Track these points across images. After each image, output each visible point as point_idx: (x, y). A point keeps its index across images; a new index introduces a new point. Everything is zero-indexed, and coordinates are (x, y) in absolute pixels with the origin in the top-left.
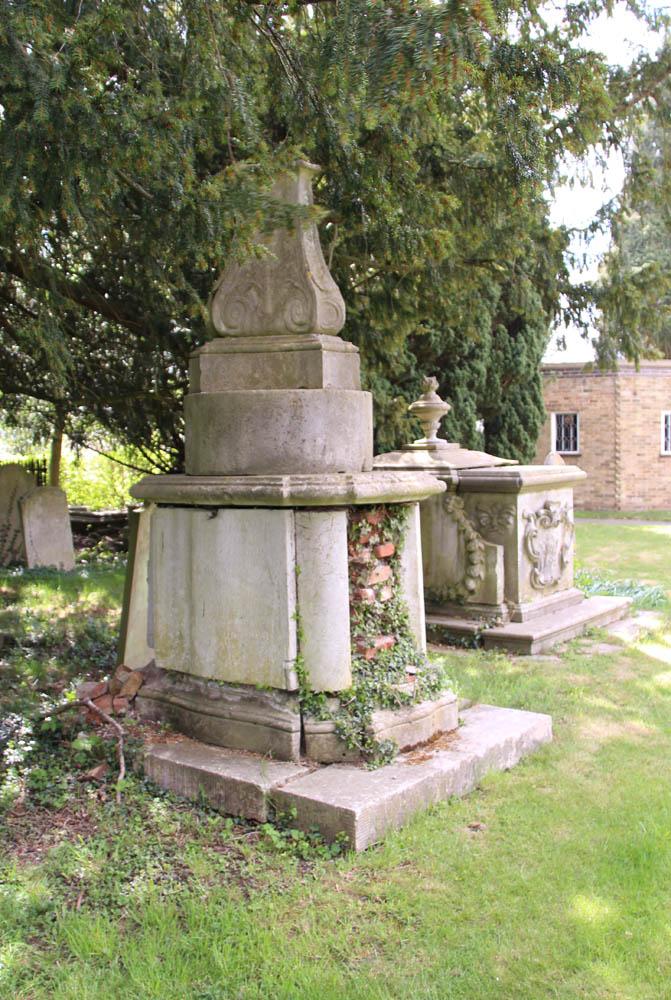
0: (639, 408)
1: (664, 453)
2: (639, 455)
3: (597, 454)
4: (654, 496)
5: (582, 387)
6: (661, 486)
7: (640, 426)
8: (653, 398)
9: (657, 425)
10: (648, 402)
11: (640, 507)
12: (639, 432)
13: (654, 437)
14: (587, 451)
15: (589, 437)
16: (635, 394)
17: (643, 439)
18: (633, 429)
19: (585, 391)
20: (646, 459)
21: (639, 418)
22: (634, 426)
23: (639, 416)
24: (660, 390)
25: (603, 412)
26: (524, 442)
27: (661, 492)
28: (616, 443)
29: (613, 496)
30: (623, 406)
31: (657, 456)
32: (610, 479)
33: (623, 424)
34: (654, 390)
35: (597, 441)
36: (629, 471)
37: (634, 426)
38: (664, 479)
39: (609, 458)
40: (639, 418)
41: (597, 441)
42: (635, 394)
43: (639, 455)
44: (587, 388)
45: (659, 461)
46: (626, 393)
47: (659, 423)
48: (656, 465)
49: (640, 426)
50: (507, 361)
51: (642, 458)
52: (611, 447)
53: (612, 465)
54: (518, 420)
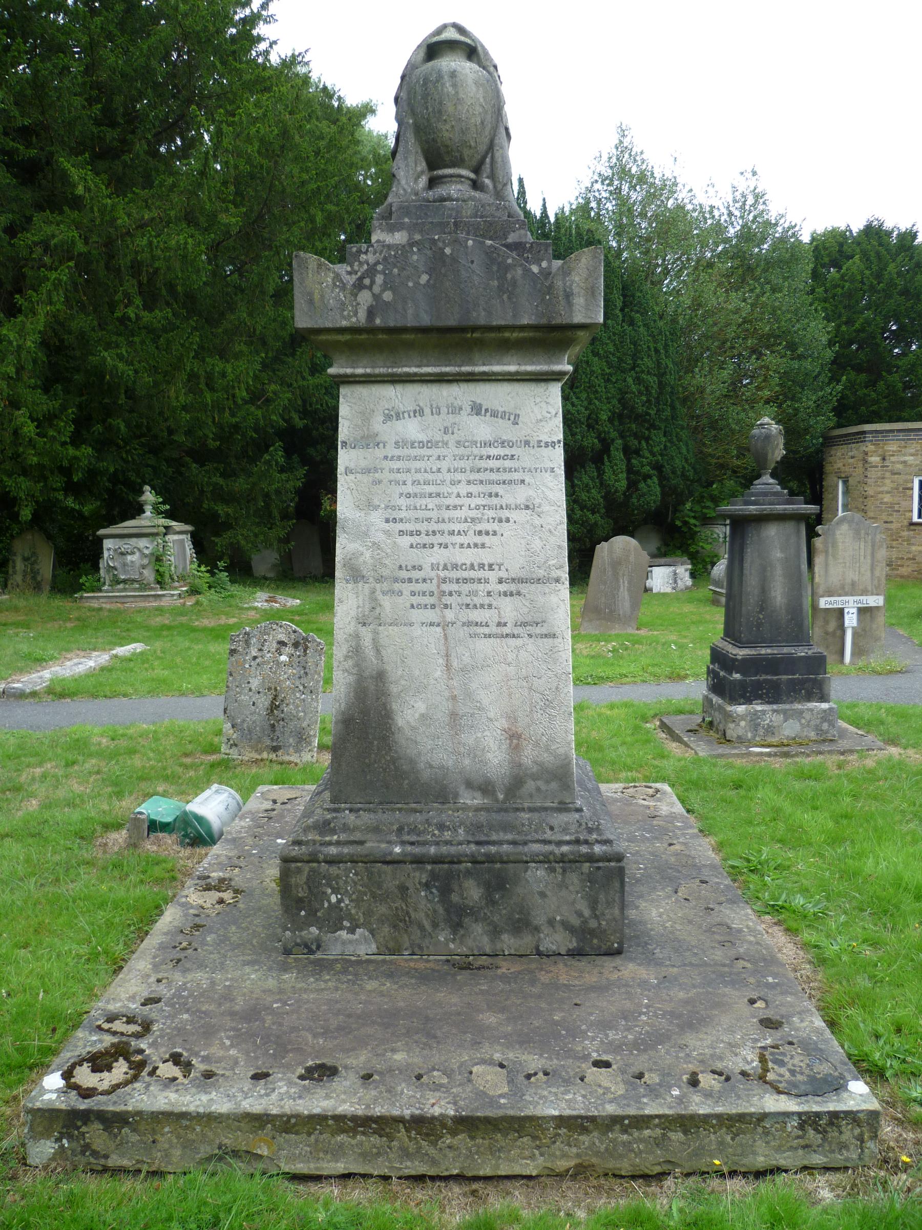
0: (888, 475)
1: (915, 519)
2: (886, 522)
4: (902, 566)
6: (911, 556)
7: (888, 492)
8: (905, 462)
10: (900, 466)
12: (887, 498)
13: (904, 503)
16: (884, 459)
17: (891, 506)
18: (880, 496)
20: (893, 526)
21: (888, 485)
22: (882, 492)
23: (887, 481)
24: (912, 455)
30: (873, 474)
31: (906, 523)
34: (905, 455)
37: (882, 492)
38: (914, 548)
40: (888, 485)
42: (884, 459)
43: (886, 522)
45: (909, 530)
46: (874, 459)
48: (905, 533)
49: (888, 492)
51: (888, 525)
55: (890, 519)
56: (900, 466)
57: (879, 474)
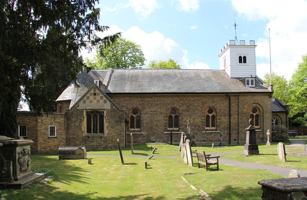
0: (43, 125)
1: (49, 136)
2: (43, 137)
3: (32, 137)
4: (47, 148)
5: (27, 119)
8: (47, 122)
9: (48, 129)
11: (43, 151)
12: (43, 131)
14: (29, 136)
15: (29, 132)
16: (42, 121)
17: (44, 133)
19: (28, 120)
21: (43, 127)
23: (43, 126)
24: (48, 120)
25: (33, 126)
26: (12, 133)
27: (49, 147)
28: (37, 134)
29: (36, 149)
30: (39, 124)
32: (35, 144)
33: (39, 129)
35: (32, 133)
36: (40, 141)
37: (42, 129)
38: (50, 144)
39: (35, 138)
40: (43, 127)
41: (32, 133)
42: (42, 121)
43: (43, 137)
44: (29, 119)
45: (48, 139)
46: (39, 121)
47: (48, 129)
48: (47, 140)
50: (7, 111)
52: (35, 135)
53: (36, 140)
54: (10, 127)
55: (44, 136)
56: (45, 123)
57: (41, 125)
